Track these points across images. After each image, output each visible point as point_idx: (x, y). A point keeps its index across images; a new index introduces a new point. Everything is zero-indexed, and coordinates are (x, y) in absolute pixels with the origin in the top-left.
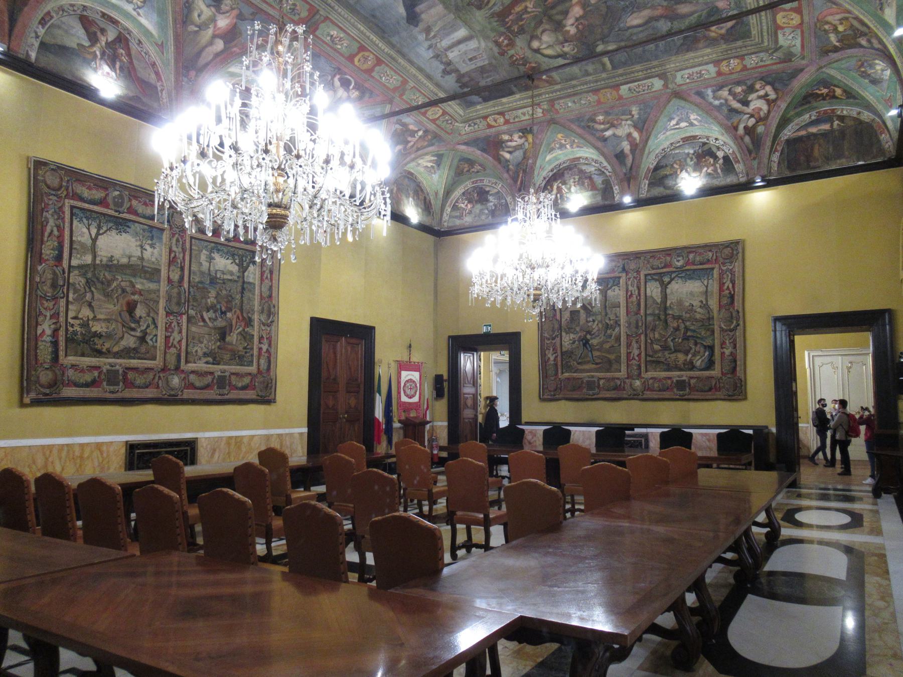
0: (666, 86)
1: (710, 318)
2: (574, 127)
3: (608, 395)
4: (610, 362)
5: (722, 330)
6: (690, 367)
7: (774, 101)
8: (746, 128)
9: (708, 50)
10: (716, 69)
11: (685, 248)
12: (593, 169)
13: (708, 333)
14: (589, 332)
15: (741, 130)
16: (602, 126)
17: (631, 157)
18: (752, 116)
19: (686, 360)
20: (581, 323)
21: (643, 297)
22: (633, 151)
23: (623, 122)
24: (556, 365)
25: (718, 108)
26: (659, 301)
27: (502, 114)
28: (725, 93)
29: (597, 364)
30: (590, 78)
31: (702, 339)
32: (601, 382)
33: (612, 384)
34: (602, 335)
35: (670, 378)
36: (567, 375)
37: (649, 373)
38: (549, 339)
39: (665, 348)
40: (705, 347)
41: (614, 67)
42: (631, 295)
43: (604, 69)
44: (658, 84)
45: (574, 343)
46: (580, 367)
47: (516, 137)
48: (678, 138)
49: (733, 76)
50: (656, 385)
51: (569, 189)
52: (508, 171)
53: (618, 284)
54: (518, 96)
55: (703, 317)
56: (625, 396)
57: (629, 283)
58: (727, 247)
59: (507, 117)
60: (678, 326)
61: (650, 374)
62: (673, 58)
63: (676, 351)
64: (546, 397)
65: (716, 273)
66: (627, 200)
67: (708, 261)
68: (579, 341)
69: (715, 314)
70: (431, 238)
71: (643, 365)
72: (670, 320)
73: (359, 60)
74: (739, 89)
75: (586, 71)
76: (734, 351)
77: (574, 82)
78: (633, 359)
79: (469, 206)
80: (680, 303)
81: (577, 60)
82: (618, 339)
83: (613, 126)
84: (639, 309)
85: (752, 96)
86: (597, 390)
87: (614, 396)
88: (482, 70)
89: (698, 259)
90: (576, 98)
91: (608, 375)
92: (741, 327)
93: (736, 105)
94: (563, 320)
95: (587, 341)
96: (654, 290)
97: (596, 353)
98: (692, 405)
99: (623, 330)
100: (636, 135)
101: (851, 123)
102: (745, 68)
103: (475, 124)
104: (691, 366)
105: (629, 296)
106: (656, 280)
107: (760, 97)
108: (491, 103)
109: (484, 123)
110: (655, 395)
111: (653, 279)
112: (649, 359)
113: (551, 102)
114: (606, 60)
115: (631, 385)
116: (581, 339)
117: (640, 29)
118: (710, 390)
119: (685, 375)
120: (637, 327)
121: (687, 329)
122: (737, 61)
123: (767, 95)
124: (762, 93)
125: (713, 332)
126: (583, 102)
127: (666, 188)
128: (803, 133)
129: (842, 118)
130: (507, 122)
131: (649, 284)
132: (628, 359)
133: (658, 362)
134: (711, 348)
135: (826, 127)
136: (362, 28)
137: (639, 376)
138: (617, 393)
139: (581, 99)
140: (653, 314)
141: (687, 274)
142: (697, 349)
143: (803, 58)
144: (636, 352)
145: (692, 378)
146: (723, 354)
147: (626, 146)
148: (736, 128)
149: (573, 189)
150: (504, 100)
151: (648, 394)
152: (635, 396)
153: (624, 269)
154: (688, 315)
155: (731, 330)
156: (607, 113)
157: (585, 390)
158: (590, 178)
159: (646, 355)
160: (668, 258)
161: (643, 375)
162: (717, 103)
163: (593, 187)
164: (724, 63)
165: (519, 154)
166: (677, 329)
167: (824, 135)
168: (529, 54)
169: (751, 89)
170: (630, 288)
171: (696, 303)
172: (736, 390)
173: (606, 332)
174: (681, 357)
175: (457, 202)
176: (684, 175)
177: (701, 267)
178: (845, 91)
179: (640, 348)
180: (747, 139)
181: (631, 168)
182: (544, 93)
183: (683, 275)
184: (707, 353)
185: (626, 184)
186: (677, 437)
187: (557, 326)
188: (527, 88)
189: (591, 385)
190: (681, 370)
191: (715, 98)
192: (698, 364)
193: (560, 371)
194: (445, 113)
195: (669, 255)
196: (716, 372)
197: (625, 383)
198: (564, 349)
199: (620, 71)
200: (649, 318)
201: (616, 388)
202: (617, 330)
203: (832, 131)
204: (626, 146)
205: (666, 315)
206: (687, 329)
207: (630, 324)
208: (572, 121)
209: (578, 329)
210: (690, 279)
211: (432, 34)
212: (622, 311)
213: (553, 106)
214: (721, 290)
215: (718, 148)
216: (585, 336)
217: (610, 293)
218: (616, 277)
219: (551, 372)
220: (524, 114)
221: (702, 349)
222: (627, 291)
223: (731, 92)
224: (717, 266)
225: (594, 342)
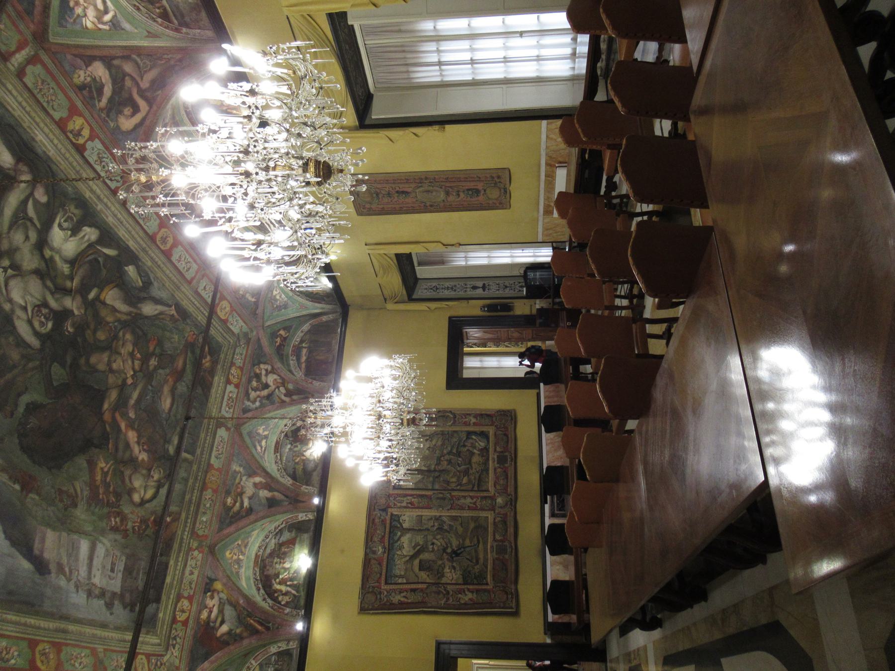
0: (228, 429)
1: (443, 433)
2: (226, 532)
3: (511, 530)
4: (476, 528)
7: (273, 368)
8: (285, 395)
9: (216, 378)
10: (232, 385)
12: (273, 541)
13: (455, 435)
14: (444, 550)
15: (287, 399)
16: (238, 504)
17: (276, 493)
18: (278, 387)
20: (434, 558)
22: (270, 489)
23: (242, 483)
24: (478, 591)
25: (262, 405)
27: (179, 597)
28: (253, 394)
30: (191, 481)
31: (460, 441)
32: (498, 537)
33: (500, 526)
35: (495, 469)
36: (489, 578)
38: (448, 599)
39: (466, 472)
40: (468, 438)
41: (193, 453)
42: (411, 503)
43: (191, 463)
44: (222, 433)
45: (454, 568)
46: (481, 561)
47: (210, 603)
48: (272, 456)
49: (244, 379)
50: (501, 482)
51: (286, 569)
52: (241, 638)
53: (398, 517)
54: (172, 562)
56: (512, 514)
57: (399, 505)
59: (186, 595)
62: (209, 405)
63: (470, 463)
64: (514, 605)
66: (316, 501)
69: (440, 429)
70: (352, 313)
71: (483, 494)
72: (440, 468)
73: (42, 662)
74: (254, 384)
75: (183, 478)
77: (187, 497)
78: (475, 503)
81: (170, 476)
82: (454, 518)
83: (241, 494)
84: (426, 496)
85: (263, 379)
86: (506, 543)
87: (512, 524)
88: (128, 571)
90: (202, 510)
91: (490, 529)
93: (265, 393)
95: (454, 552)
97: (467, 543)
98: (520, 454)
99: (445, 514)
100: (258, 479)
101: (308, 337)
102: (241, 369)
103: (175, 638)
104: (485, 450)
105: (412, 506)
107: (266, 375)
108: (164, 597)
109: (179, 626)
112: (476, 488)
113: (193, 533)
114: (184, 455)
115: (501, 507)
116: (451, 560)
117: (175, 406)
119: (493, 456)
120: (444, 499)
122: (233, 368)
123: (266, 370)
124: (264, 372)
126: (208, 505)
127: (314, 470)
128: (303, 366)
129: (302, 341)
130: (190, 598)
132: (475, 509)
133: (480, 477)
134: (469, 434)
135: (304, 351)
136: (14, 618)
137: (493, 498)
138: (509, 524)
139: (205, 505)
140: (433, 483)
143: (252, 331)
144: (469, 500)
145: (495, 450)
146: (475, 424)
147: (264, 494)
148: (283, 402)
149: (287, 565)
150: (168, 580)
151: (510, 489)
152: (513, 502)
155: (455, 417)
156: (228, 493)
157: (507, 557)
158: (281, 545)
162: (258, 404)
163: (292, 543)
164: (231, 377)
165: (229, 612)
167: (310, 351)
168: (141, 512)
169: (258, 377)
170: (404, 504)
172: (507, 418)
173: (446, 531)
174: (475, 459)
176: (307, 454)
178: (284, 329)
180: (295, 397)
181: (287, 497)
182: (182, 533)
185: (301, 505)
186: (555, 541)
187: (434, 588)
188: (168, 546)
189: (501, 550)
190: (488, 459)
191: (254, 402)
192: (482, 444)
193: (484, 587)
194: (148, 656)
196: (491, 431)
198: (461, 581)
199: (199, 451)
200: (437, 487)
201: (504, 522)
202: (445, 519)
203: (309, 348)
204: (264, 494)
205: (435, 471)
206: (450, 453)
207: (440, 506)
208: (220, 530)
209: (440, 562)
211: (67, 569)
212: (426, 513)
213: (198, 536)
215: (293, 425)
216: (447, 553)
217: (405, 525)
218: (391, 519)
220: (192, 573)
221: (471, 441)
222: (405, 507)
223: (255, 389)
225: (455, 543)
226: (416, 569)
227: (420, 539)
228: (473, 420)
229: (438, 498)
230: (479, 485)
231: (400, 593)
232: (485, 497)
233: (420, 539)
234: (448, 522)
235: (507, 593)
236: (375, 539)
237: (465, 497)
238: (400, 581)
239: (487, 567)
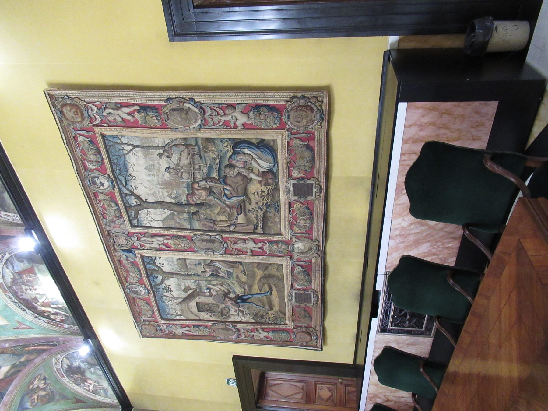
4: (267, 277)
5: (204, 125)
6: (270, 176)
11: (79, 173)
19: (260, 182)
21: (166, 232)
24: (274, 331)
26: (168, 212)
29: (271, 289)
34: (229, 282)
35: (291, 205)
37: (283, 231)
39: (241, 208)
42: (167, 245)
46: (276, 308)
50: (302, 223)
53: (153, 260)
55: (185, 155)
56: (319, 261)
58: (62, 112)
60: (205, 189)
61: (284, 228)
63: (245, 193)
65: (108, 132)
67: (92, 142)
68: (239, 307)
72: (196, 200)
76: (239, 108)
78: (261, 248)
79: (90, 382)
80: (166, 185)
82: (232, 264)
84: (185, 237)
87: (319, 275)
89: (93, 157)
92: (198, 96)
94: (211, 319)
95: (238, 297)
96: (153, 218)
98: (335, 173)
104: (269, 175)
106: (137, 214)
110: (318, 224)
111: (136, 217)
115: (302, 253)
118: (311, 149)
121: (208, 178)
125: (209, 140)
131: (145, 223)
134: (237, 144)
141: (119, 174)
142: (240, 164)
144: (251, 245)
145: (289, 176)
146: (245, 126)
151: (317, 234)
153: (129, 251)
154: (185, 175)
157: (310, 305)
158: (20, 273)
159: (254, 233)
160: (101, 197)
161: (287, 239)
166: (210, 191)
170: (155, 245)
171: (164, 163)
172: (314, 104)
174: (254, 188)
175: (89, 391)
177: (104, 153)
179: (245, 240)
183: (122, 179)
184: (246, 151)
187: (221, 326)
189: (302, 297)
190: (277, 189)
192: (265, 165)
195: (95, 195)
196: (280, 139)
197: (298, 260)
200: (197, 225)
202: (218, 265)
206: (208, 178)
207: (208, 250)
210: (127, 170)
214: (135, 125)
219: (284, 336)
221: (241, 157)
224: (97, 130)
226: (195, 310)
227: (190, 283)
229: (204, 241)
230: (264, 225)
232: (276, 242)
233: (190, 283)
234: (223, 268)
235: (309, 334)
236: (130, 280)
238: (178, 318)
239: (284, 314)
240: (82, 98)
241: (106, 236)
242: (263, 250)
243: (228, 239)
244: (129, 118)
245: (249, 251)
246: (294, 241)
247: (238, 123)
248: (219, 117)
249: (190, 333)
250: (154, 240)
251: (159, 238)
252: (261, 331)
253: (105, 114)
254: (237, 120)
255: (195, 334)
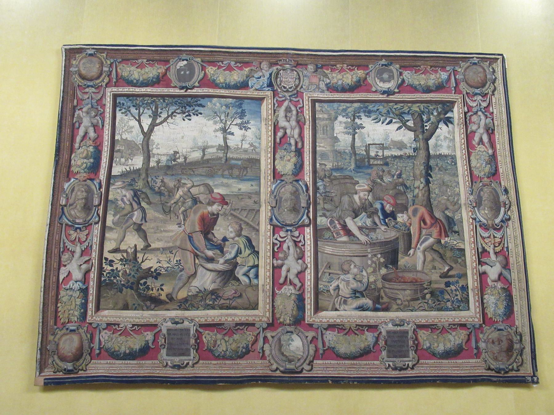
92: (514, 224)
144: (296, 267)
146: (483, 276)
170: (283, 123)
222: (276, 128)
228: (493, 272)
231: (95, 126)
237: (301, 257)
240: (496, 93)
241: (298, 59)
242: (285, 283)
243: (302, 233)
244: (477, 139)
245: (280, 262)
246: (307, 334)
247: (485, 268)
248: (492, 246)
249: (78, 139)
250: (294, 123)
251: (297, 131)
252: (84, 267)
253: (480, 113)
254: (492, 267)
255: (77, 145)
